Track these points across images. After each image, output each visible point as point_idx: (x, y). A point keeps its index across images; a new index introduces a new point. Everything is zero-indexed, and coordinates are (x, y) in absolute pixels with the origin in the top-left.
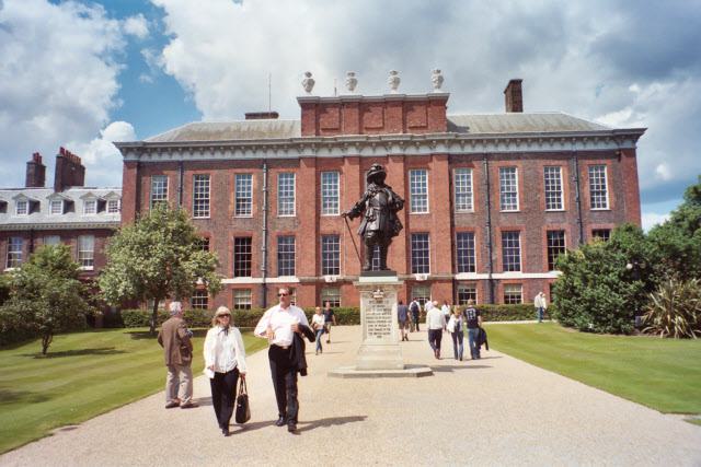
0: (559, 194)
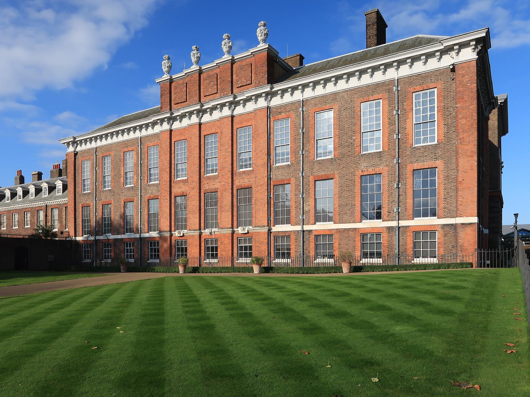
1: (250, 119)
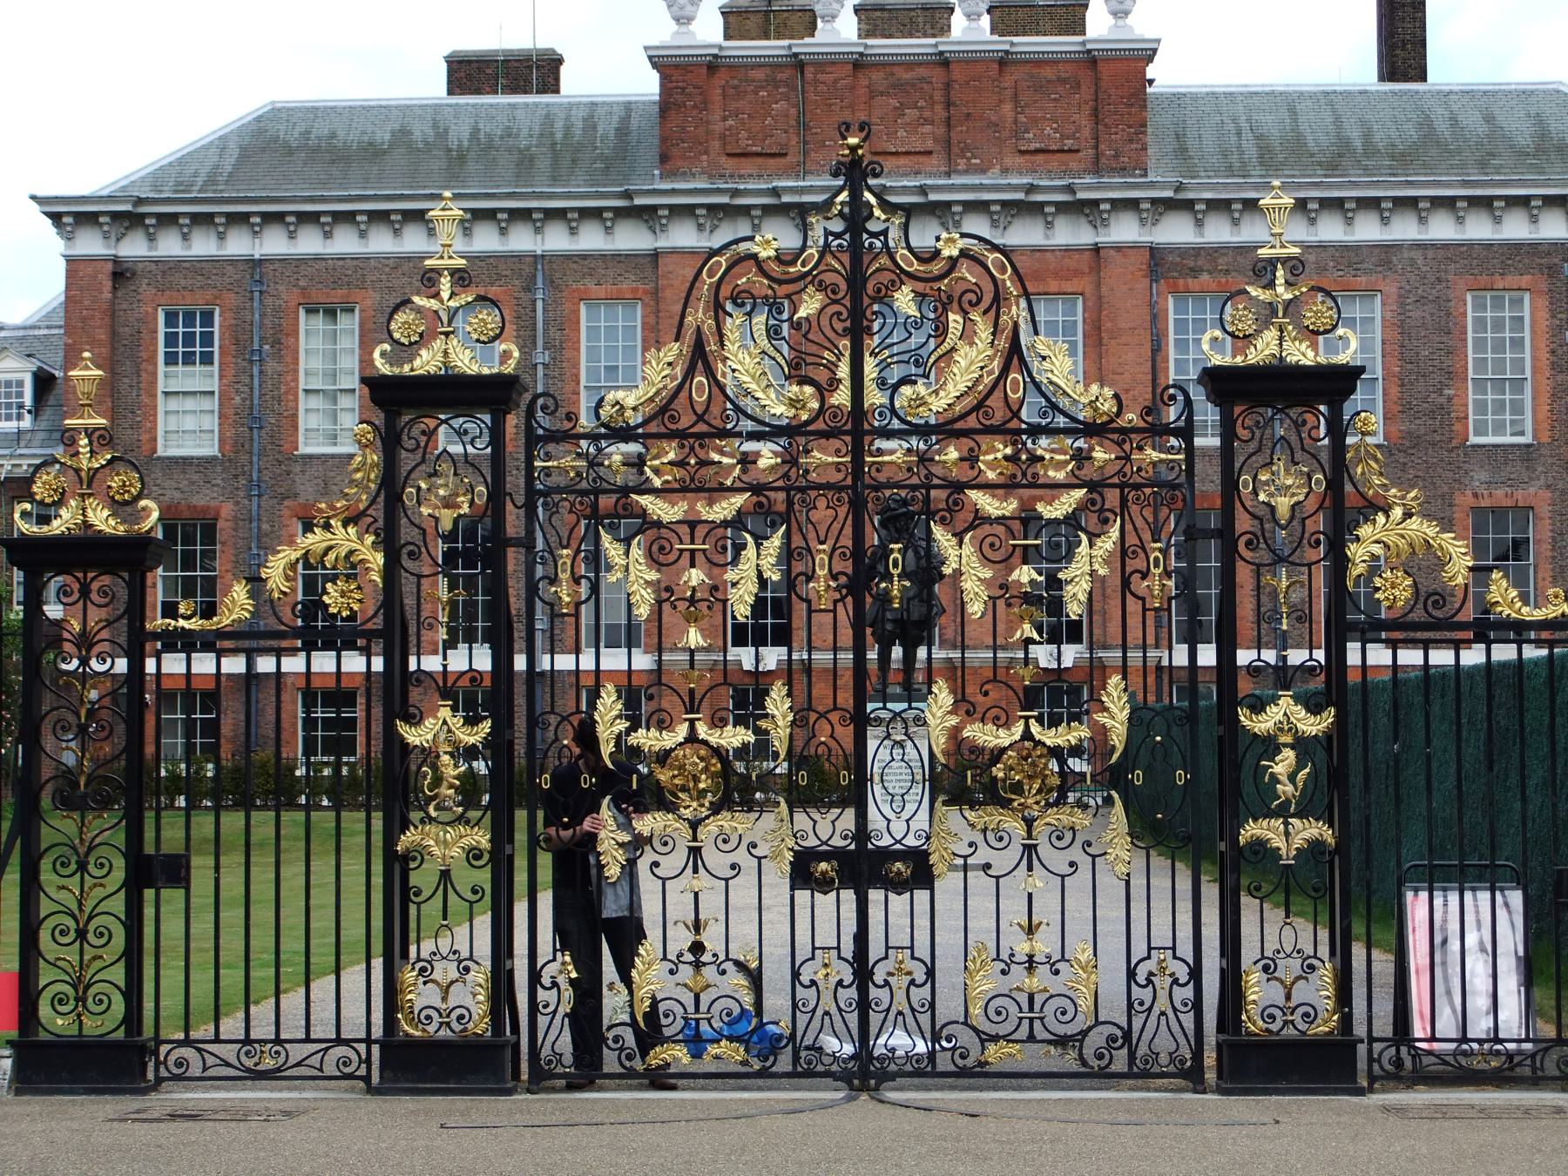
0: (1518, 384)
1: (1077, 273)
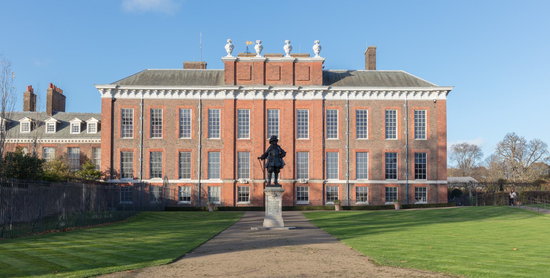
1: (308, 105)
